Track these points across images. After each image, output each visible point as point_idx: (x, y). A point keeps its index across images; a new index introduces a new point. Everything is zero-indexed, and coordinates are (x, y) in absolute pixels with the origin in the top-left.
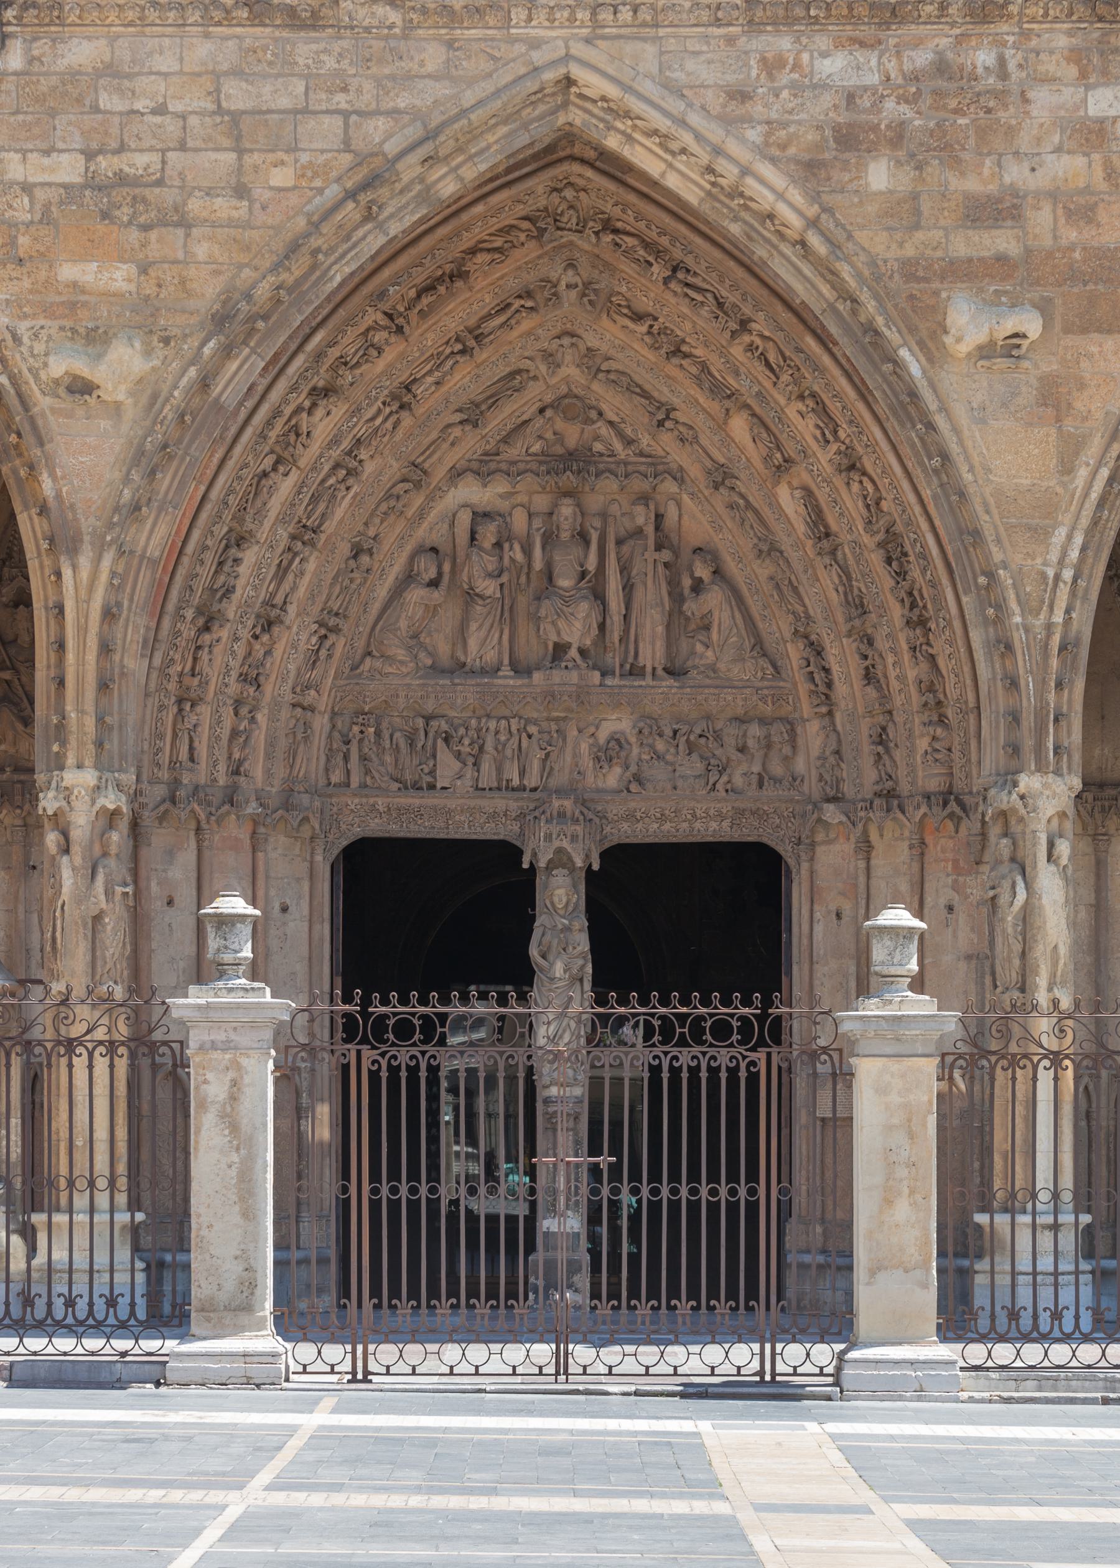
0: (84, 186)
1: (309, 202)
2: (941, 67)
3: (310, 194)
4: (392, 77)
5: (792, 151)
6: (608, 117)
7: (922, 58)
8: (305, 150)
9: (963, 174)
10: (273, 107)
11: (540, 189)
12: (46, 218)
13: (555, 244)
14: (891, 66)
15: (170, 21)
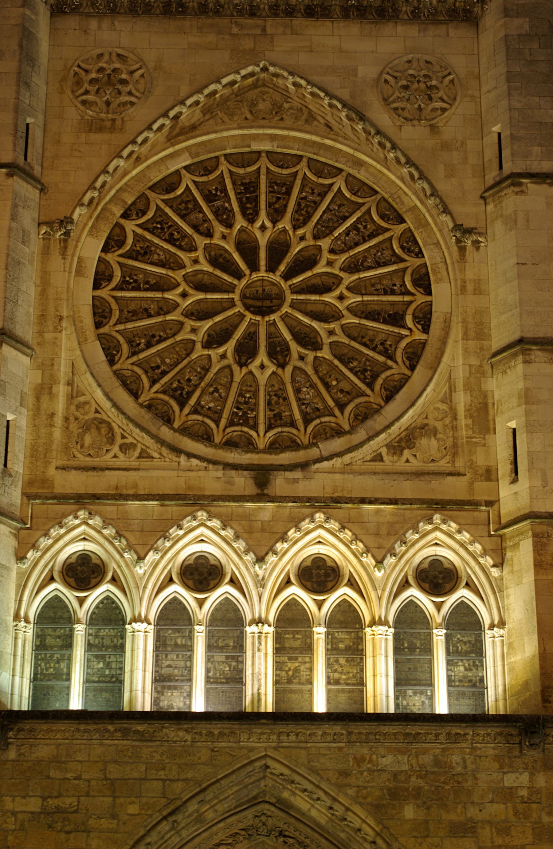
0: (41, 813)
1: (146, 821)
2: (437, 763)
3: (146, 817)
4: (186, 764)
5: (369, 800)
6: (284, 783)
7: (427, 759)
8: (144, 797)
9: (448, 812)
10: (130, 777)
11: (250, 816)
12: (22, 828)
13: (256, 842)
14: (414, 761)
15: (85, 738)
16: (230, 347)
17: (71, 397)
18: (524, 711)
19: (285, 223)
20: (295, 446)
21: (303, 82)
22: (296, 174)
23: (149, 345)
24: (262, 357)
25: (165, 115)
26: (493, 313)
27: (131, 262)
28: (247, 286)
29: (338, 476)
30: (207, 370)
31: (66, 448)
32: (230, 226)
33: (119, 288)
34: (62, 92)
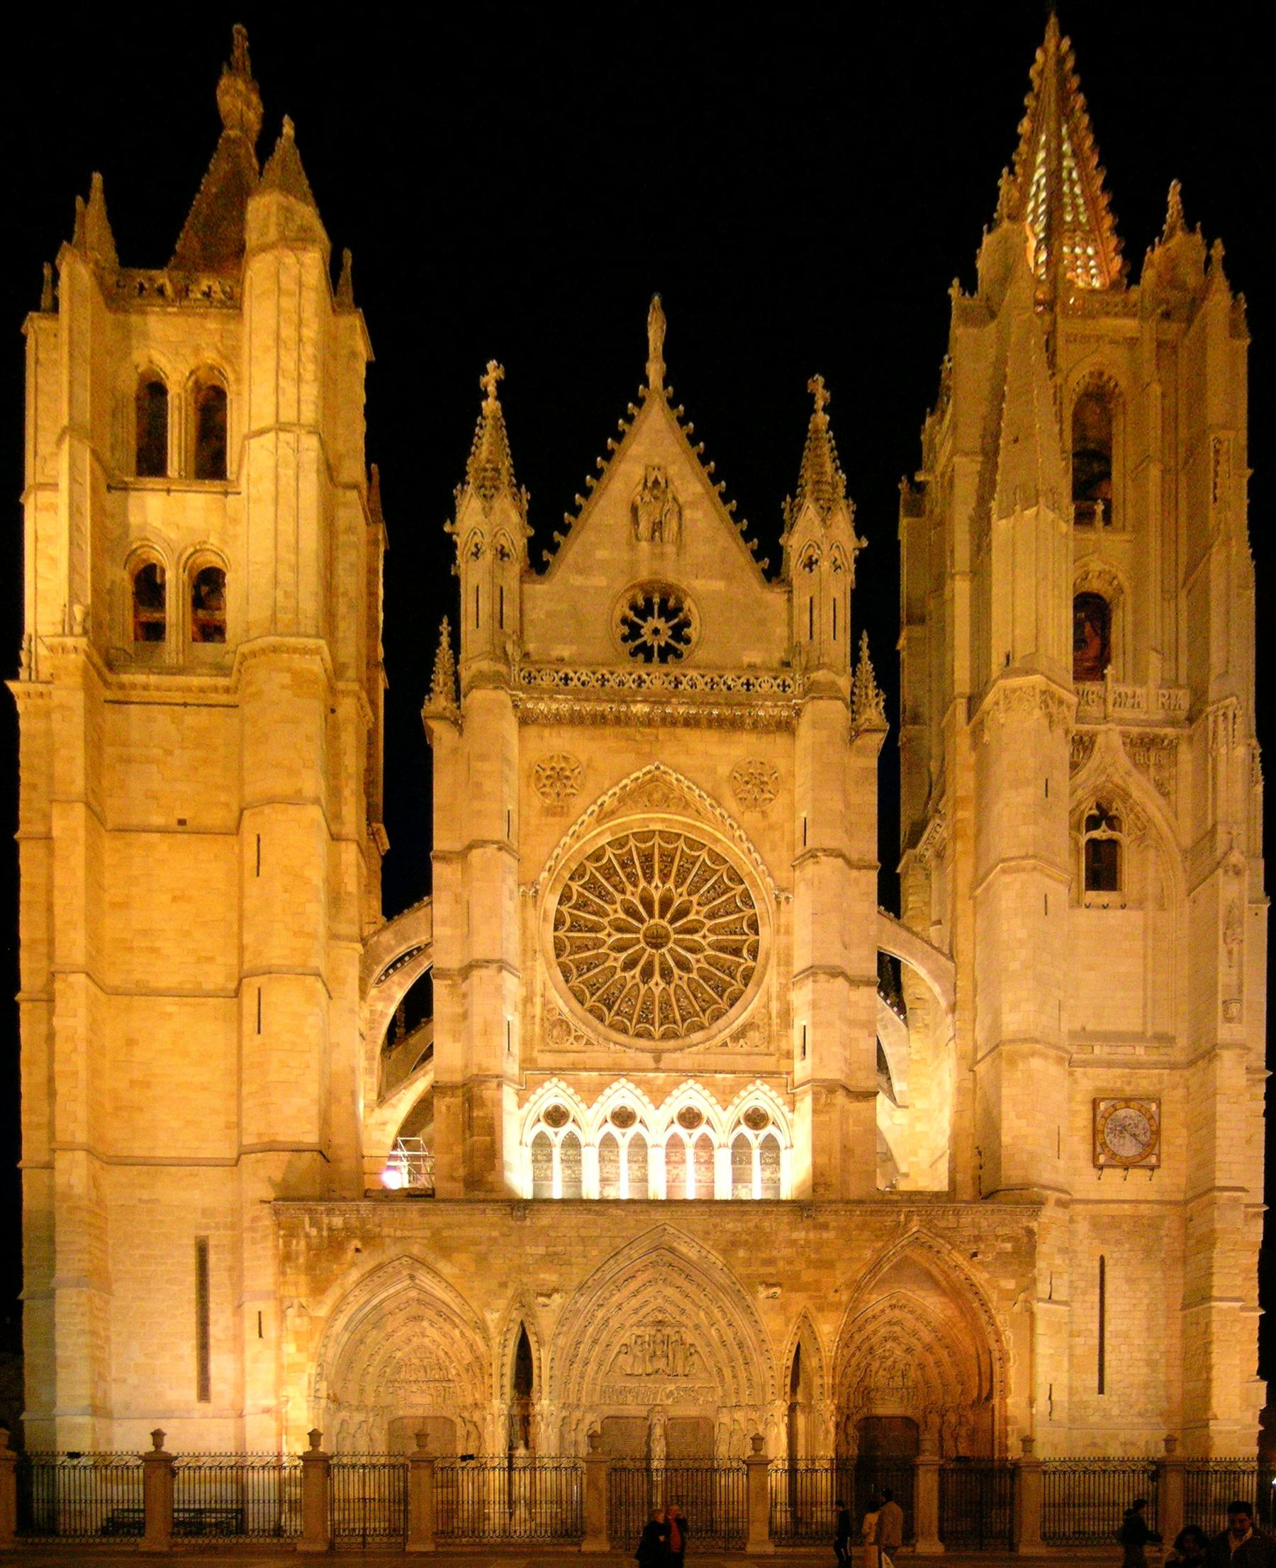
16: (637, 971)
17: (544, 1005)
18: (802, 1197)
19: (670, 885)
20: (676, 1036)
21: (682, 778)
22: (676, 848)
23: (589, 970)
24: (657, 977)
25: (594, 802)
26: (796, 948)
27: (576, 912)
28: (648, 929)
29: (701, 1057)
30: (623, 986)
31: (543, 1038)
32: (636, 886)
33: (569, 930)
34: (528, 786)
